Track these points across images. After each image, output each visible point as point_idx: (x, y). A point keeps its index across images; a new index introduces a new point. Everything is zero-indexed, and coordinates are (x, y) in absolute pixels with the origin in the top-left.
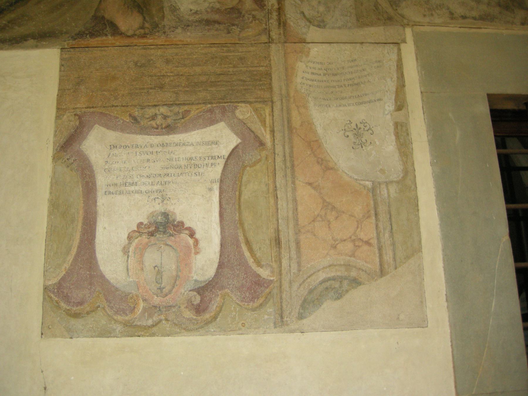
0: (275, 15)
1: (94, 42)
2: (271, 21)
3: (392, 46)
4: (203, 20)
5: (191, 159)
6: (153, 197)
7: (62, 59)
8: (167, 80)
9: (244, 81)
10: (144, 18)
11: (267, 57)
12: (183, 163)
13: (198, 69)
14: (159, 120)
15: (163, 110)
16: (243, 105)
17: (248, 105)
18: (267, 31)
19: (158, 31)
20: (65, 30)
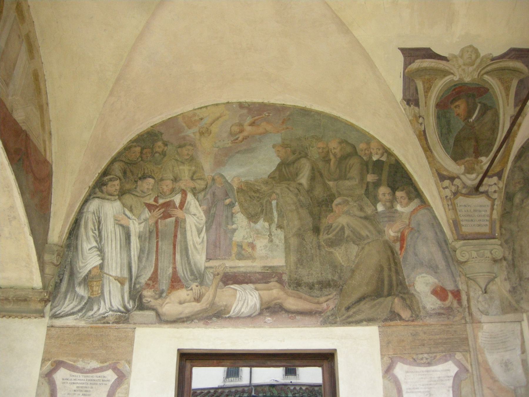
0: (467, 310)
1: (392, 323)
2: (465, 313)
3: (518, 323)
4: (437, 313)
5: (439, 377)
6: (426, 394)
7: (379, 331)
8: (425, 342)
9: (457, 342)
10: (412, 312)
11: (466, 330)
12: (437, 379)
13: (438, 337)
14: (424, 360)
15: (426, 355)
16: (458, 353)
17: (460, 353)
18: (464, 318)
19: (419, 319)
20: (379, 318)
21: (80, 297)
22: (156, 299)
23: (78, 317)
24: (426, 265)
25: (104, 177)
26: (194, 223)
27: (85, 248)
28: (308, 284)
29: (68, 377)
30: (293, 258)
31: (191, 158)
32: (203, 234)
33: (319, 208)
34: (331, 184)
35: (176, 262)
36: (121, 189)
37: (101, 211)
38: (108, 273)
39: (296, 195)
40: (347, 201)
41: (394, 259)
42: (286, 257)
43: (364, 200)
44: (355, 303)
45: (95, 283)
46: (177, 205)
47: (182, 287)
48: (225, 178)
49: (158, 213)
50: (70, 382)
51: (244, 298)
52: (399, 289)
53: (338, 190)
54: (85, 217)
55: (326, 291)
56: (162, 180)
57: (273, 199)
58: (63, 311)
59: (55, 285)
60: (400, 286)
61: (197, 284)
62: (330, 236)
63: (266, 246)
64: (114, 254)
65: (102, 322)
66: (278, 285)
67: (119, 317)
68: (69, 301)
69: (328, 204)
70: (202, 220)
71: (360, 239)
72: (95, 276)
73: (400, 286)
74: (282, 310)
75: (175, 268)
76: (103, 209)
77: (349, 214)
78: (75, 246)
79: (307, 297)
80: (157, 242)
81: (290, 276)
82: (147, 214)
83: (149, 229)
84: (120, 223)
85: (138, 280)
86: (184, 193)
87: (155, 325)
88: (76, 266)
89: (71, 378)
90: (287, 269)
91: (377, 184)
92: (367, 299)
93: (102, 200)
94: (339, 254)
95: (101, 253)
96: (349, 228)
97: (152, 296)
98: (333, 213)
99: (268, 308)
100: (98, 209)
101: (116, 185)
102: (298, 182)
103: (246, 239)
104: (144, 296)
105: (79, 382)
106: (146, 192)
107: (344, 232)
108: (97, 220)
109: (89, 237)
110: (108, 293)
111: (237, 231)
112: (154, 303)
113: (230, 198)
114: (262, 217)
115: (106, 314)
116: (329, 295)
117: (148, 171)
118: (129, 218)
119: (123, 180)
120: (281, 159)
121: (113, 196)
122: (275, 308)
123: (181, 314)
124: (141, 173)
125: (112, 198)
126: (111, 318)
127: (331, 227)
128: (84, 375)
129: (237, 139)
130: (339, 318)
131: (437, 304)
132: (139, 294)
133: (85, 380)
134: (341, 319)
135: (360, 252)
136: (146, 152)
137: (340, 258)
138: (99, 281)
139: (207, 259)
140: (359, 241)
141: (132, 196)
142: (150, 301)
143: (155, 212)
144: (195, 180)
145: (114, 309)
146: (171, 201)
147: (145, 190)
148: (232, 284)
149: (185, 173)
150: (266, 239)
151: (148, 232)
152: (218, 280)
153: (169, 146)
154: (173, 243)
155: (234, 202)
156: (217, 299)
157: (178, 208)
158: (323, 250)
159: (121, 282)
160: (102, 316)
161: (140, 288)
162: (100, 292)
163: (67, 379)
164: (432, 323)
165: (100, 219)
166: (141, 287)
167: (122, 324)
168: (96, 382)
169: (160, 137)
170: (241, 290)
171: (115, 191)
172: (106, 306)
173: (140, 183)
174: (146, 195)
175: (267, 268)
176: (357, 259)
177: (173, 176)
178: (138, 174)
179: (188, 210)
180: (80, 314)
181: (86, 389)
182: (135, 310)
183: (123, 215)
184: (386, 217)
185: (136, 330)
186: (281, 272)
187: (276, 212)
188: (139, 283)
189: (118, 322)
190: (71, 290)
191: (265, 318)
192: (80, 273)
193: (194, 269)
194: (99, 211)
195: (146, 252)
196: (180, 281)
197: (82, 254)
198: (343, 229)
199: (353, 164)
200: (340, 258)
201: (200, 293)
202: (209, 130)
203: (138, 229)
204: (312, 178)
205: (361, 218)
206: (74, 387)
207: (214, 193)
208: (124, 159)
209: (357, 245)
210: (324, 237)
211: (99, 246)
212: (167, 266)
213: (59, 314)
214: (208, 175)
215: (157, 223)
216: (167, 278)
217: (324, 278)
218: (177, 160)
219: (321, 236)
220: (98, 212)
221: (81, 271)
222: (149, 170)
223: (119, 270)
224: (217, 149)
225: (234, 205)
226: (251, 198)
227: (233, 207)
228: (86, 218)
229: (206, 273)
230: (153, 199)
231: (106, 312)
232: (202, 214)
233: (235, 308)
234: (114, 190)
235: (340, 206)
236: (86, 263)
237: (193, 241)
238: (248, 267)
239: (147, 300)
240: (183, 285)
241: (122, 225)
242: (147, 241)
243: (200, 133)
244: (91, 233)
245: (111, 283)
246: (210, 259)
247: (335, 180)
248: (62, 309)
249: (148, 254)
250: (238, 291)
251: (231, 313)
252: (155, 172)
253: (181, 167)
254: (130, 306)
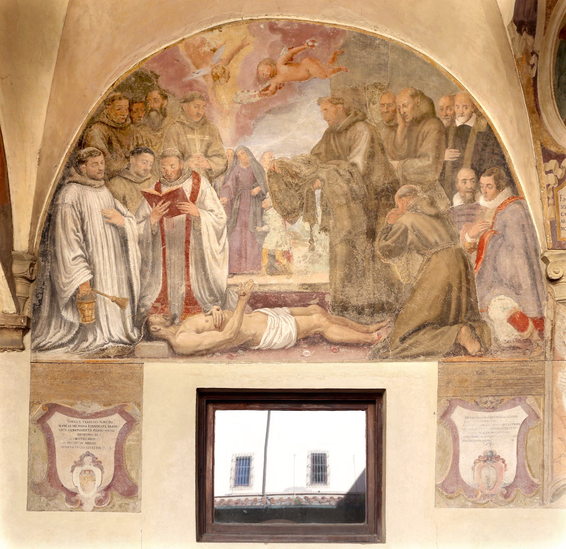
4: (511, 346)
5: (504, 424)
6: (486, 443)
8: (493, 382)
9: (531, 383)
12: (500, 427)
14: (489, 404)
15: (491, 398)
16: (530, 396)
17: (532, 397)
21: (69, 324)
22: (167, 327)
23: (69, 350)
24: (506, 284)
25: (81, 149)
26: (212, 223)
27: (67, 258)
28: (357, 308)
29: (66, 423)
30: (339, 273)
31: (203, 120)
32: (224, 238)
33: (376, 201)
34: (395, 164)
35: (190, 278)
36: (107, 169)
37: (82, 204)
38: (101, 292)
39: (348, 181)
40: (415, 190)
41: (467, 275)
42: (331, 271)
43: (437, 189)
44: (412, 333)
45: (86, 306)
46: (188, 195)
47: (199, 311)
48: (251, 154)
49: (162, 208)
50: (69, 428)
51: (277, 325)
52: (469, 315)
53: (405, 173)
54: (61, 212)
55: (377, 318)
56: (164, 156)
57: (317, 188)
58: (49, 342)
59: (34, 308)
60: (470, 312)
61: (218, 307)
62: (389, 242)
63: (305, 257)
64: (108, 267)
65: (101, 355)
66: (319, 309)
67: (122, 349)
68: (55, 329)
69: (390, 196)
70: (221, 218)
71: (426, 246)
72: (86, 295)
73: (470, 312)
74: (323, 341)
75: (189, 286)
76: (85, 200)
77: (416, 211)
78: (53, 254)
79: (354, 324)
80: (164, 250)
81: (335, 297)
82: (147, 209)
83: (152, 231)
84: (110, 221)
85: (142, 302)
86: (196, 176)
87: (167, 360)
88: (59, 283)
89: (69, 424)
90: (331, 288)
91: (457, 165)
92: (428, 328)
93: (82, 186)
94: (398, 267)
95: (90, 264)
96: (414, 231)
97: (161, 323)
98: (395, 209)
99: (305, 339)
100: (77, 200)
101: (100, 163)
102: (351, 161)
103: (281, 246)
104: (151, 322)
105: (79, 428)
106: (143, 175)
107: (407, 237)
108: (79, 216)
109: (71, 242)
110: (105, 319)
111: (268, 235)
112: (164, 332)
113: (258, 185)
114: (302, 215)
115: (105, 346)
116: (382, 322)
117: (143, 141)
118: (123, 215)
119: (109, 156)
120: (329, 124)
121: (97, 180)
122: (314, 338)
123: (199, 345)
124: (133, 144)
125: (97, 183)
126: (112, 351)
127: (391, 229)
128: (85, 420)
129: (267, 89)
130: (392, 351)
131: (513, 335)
132: (145, 320)
133: (88, 426)
134: (394, 352)
135: (425, 265)
136: (137, 109)
137: (398, 273)
138: (91, 303)
139: (230, 273)
140: (425, 250)
141: (124, 181)
142: (160, 329)
143: (158, 206)
144: (211, 157)
145: (115, 339)
146: (178, 189)
147: (142, 172)
148: (262, 307)
149: (195, 145)
150: (306, 246)
151: (150, 235)
152: (245, 302)
153: (169, 98)
154: (185, 252)
155: (264, 192)
156: (243, 327)
157: (189, 201)
158: (378, 261)
159: (121, 304)
160: (100, 348)
161: (145, 313)
162: (94, 317)
163: (65, 426)
164: (504, 359)
165: (83, 214)
166: (146, 310)
167: (127, 359)
168: (101, 428)
169: (155, 83)
170: (273, 316)
171: (99, 173)
172: (103, 335)
173: (133, 159)
174: (143, 179)
175: (307, 287)
176: (420, 274)
177: (180, 151)
178: (129, 146)
179: (203, 203)
180: (72, 346)
181: (89, 437)
182: (142, 341)
183: (115, 210)
184: (463, 215)
185: (144, 365)
186: (324, 292)
187: (319, 207)
188: (144, 306)
189: (121, 356)
190: (55, 314)
191: (302, 351)
192: (65, 292)
193: (213, 287)
194: (80, 204)
195: (150, 264)
196: (196, 303)
197: (64, 266)
198: (405, 232)
199: (428, 133)
200: (398, 273)
201: (222, 319)
202: (227, 72)
203: (136, 231)
204: (370, 156)
205: (430, 216)
206: (75, 435)
207: (237, 178)
208: (105, 120)
209: (422, 255)
210: (380, 243)
211: (85, 254)
212: (178, 284)
213: (44, 345)
214: (229, 150)
215: (161, 222)
216: (180, 299)
217: (377, 300)
218: (182, 124)
219: (376, 243)
220: (78, 205)
221: (65, 289)
222: (144, 139)
223: (116, 288)
224: (239, 106)
225: (264, 197)
226: (286, 185)
227: (263, 200)
228: (63, 213)
229: (229, 293)
230: (154, 186)
231: (105, 344)
232: (222, 209)
233: (266, 338)
234: (98, 171)
235: (404, 198)
236: (71, 279)
237: (211, 249)
238: (283, 284)
239: (156, 328)
240: (201, 308)
241: (114, 225)
242: (151, 248)
243: (213, 77)
244: (72, 236)
245: (107, 305)
246: (234, 274)
247: (401, 158)
248: (47, 340)
249: (153, 267)
250: (269, 317)
251: (261, 344)
252: (154, 144)
253: (189, 136)
254: (135, 335)
